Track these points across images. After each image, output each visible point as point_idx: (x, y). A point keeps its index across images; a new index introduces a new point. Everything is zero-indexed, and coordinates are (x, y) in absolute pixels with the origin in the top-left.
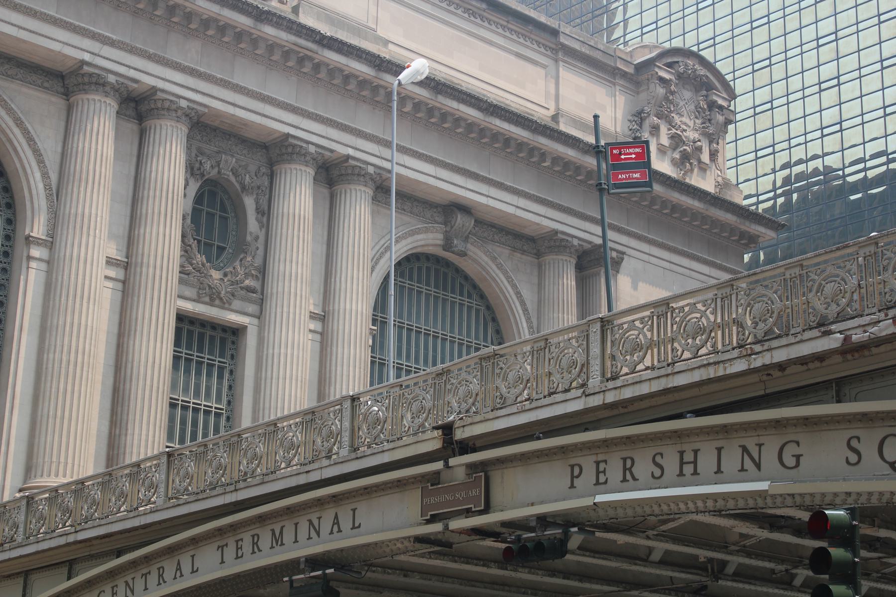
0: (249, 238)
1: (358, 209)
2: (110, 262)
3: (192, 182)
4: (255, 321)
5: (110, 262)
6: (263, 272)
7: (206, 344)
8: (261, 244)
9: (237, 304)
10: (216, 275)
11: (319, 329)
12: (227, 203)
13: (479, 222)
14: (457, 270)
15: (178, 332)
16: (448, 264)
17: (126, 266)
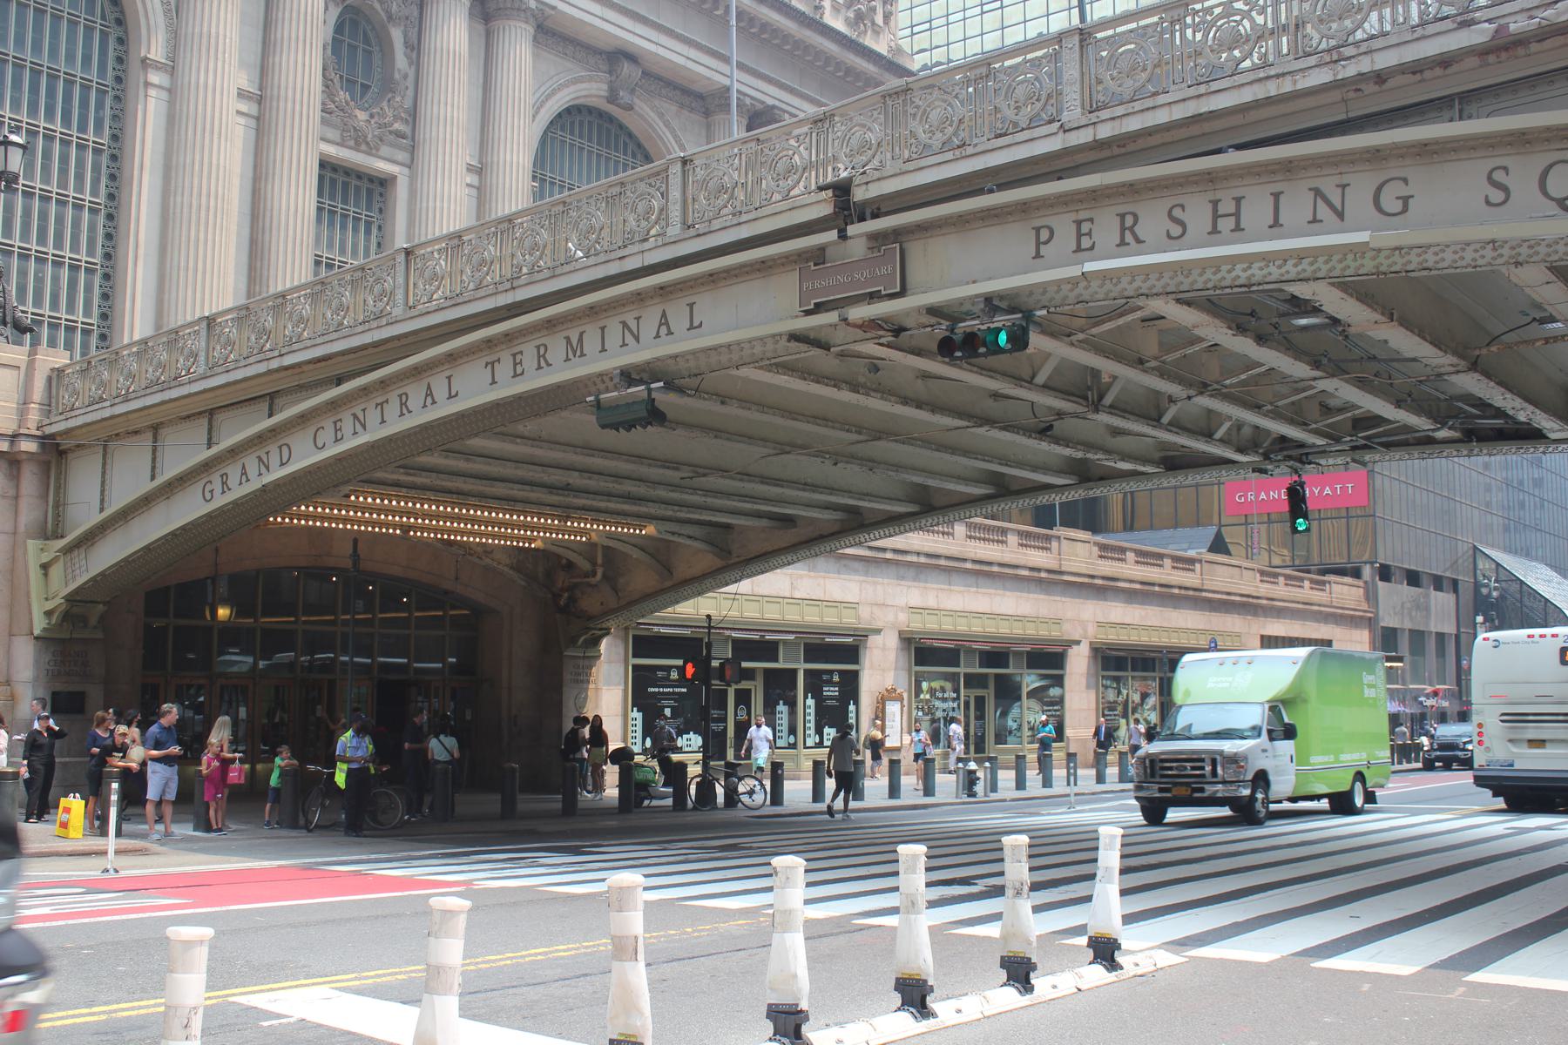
0: (397, 76)
1: (518, 51)
2: (242, 94)
3: (331, 6)
4: (406, 171)
5: (242, 94)
6: (413, 115)
7: (351, 192)
8: (410, 82)
9: (385, 150)
10: (362, 116)
11: (476, 183)
12: (371, 34)
13: (646, 74)
14: (621, 126)
15: (321, 178)
16: (611, 119)
17: (260, 100)
